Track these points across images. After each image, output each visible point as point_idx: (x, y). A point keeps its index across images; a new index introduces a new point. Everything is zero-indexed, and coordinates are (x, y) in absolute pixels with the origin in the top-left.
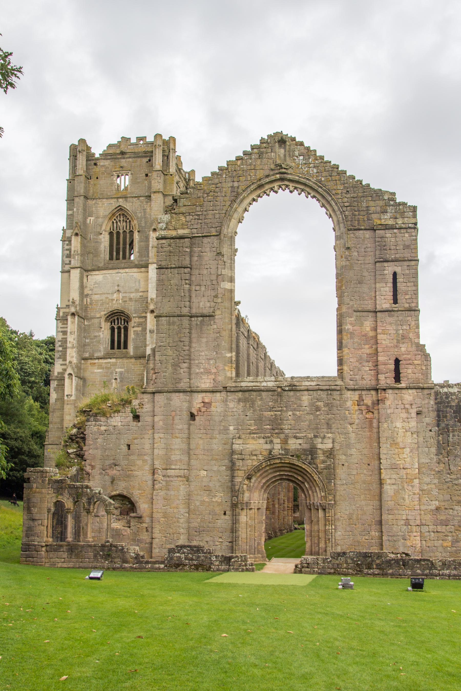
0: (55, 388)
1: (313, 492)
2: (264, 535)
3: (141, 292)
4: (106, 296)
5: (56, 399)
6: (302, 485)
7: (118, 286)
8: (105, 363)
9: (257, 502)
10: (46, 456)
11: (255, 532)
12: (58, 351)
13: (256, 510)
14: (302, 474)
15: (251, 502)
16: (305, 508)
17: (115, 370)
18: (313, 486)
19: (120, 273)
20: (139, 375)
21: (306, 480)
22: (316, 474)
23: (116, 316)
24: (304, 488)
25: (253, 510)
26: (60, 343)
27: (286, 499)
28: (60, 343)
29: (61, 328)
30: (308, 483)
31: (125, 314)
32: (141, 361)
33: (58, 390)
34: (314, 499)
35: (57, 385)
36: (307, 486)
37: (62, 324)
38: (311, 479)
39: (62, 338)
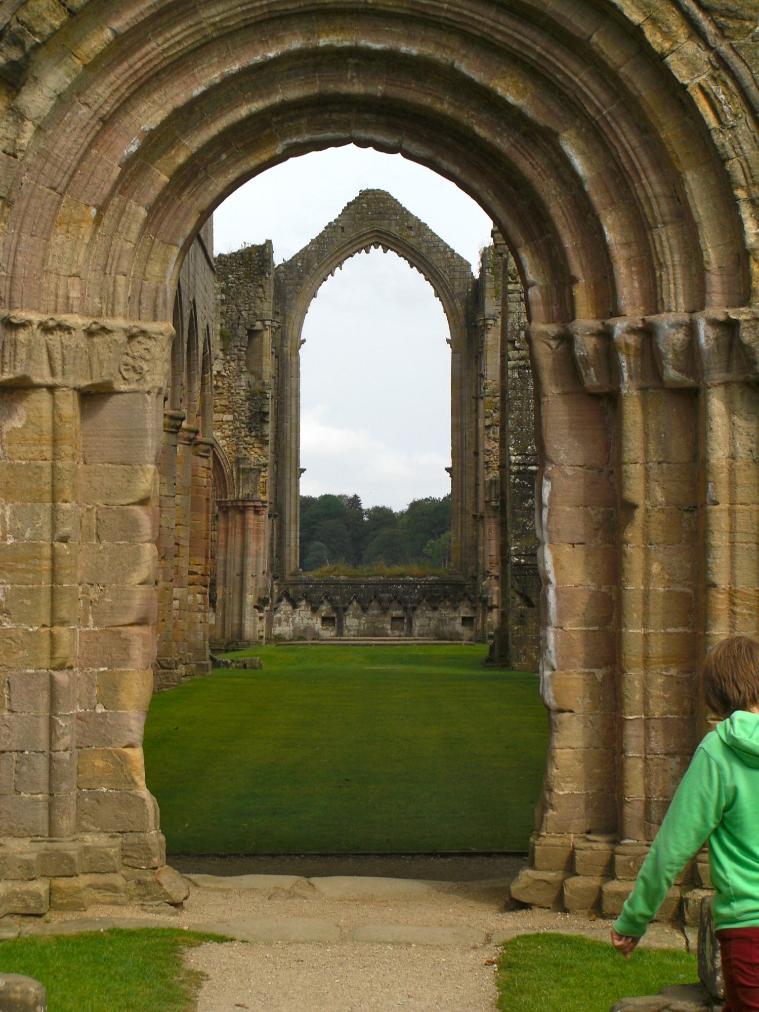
1: (640, 228)
2: (141, 646)
6: (529, 166)
9: (75, 320)
11: (55, 620)
13: (69, 406)
14: (537, 44)
15: (20, 315)
16: (551, 390)
18: (643, 160)
21: (572, 106)
22: (696, 32)
24: (550, 192)
25: (41, 401)
27: (183, 534)
30: (596, 136)
34: (653, 301)
36: (579, 164)
38: (640, 85)
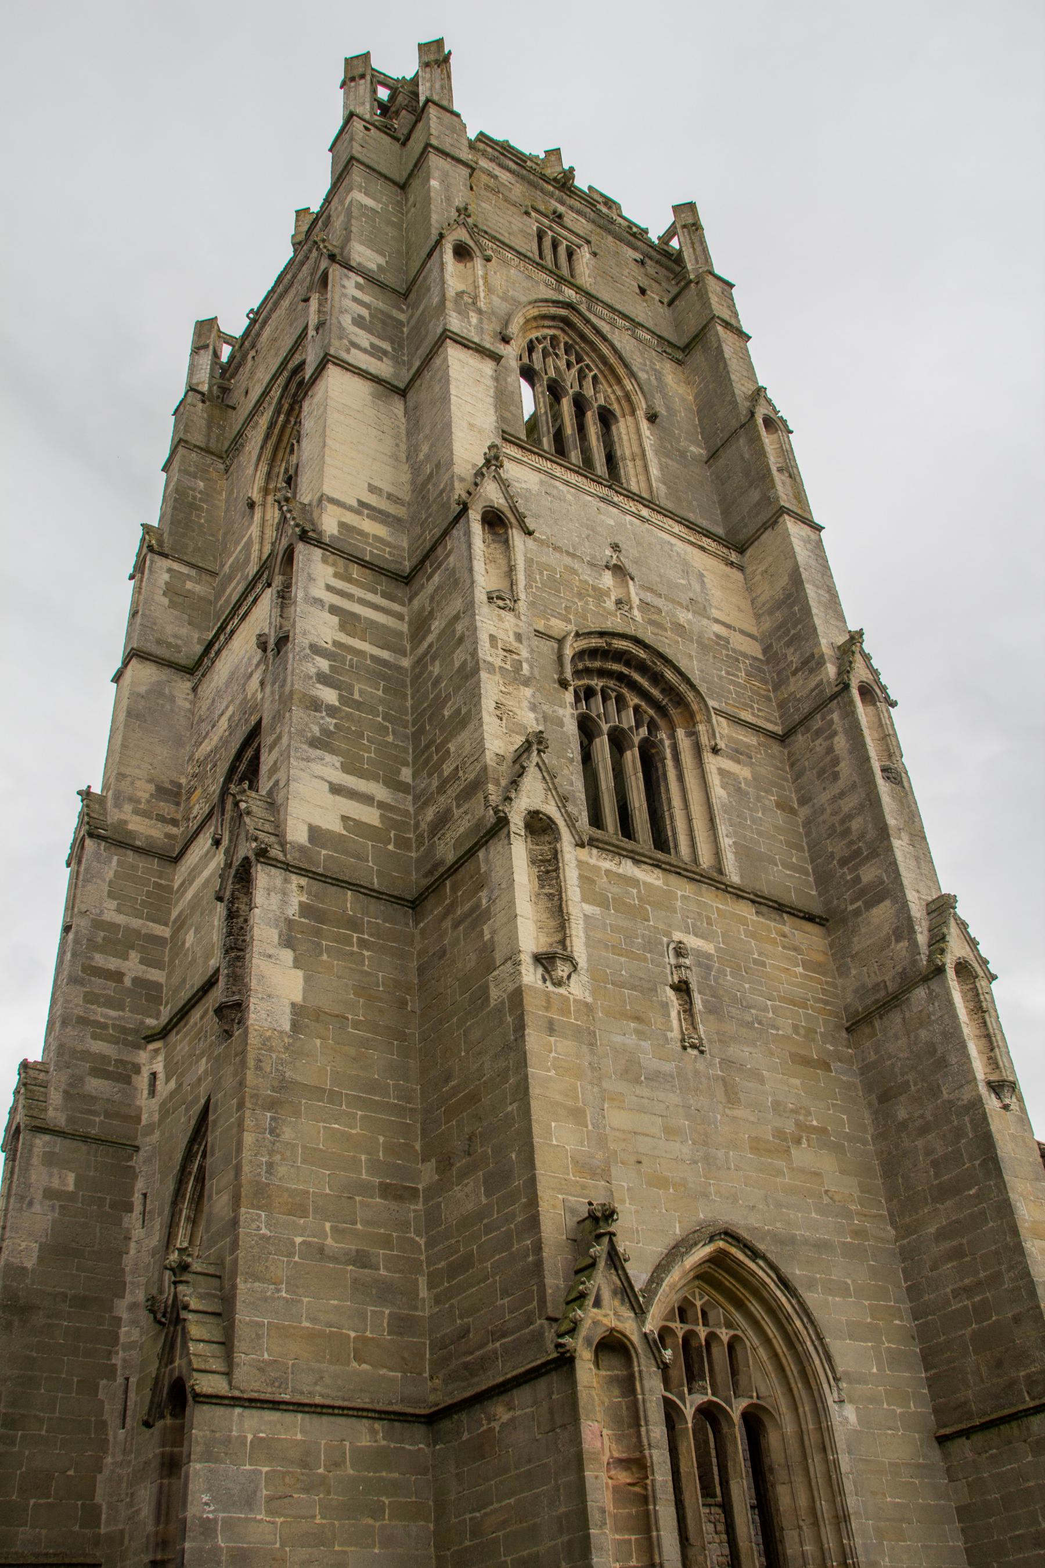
0: (289, 922)
3: (717, 621)
4: (568, 560)
5: (298, 1011)
7: (616, 547)
8: (608, 872)
10: (208, 1528)
12: (316, 705)
17: (668, 934)
19: (615, 505)
20: (793, 1003)
23: (602, 673)
26: (324, 664)
28: (324, 664)
29: (329, 588)
31: (657, 678)
32: (786, 929)
33: (318, 949)
35: (305, 909)
37: (336, 575)
39: (335, 643)
